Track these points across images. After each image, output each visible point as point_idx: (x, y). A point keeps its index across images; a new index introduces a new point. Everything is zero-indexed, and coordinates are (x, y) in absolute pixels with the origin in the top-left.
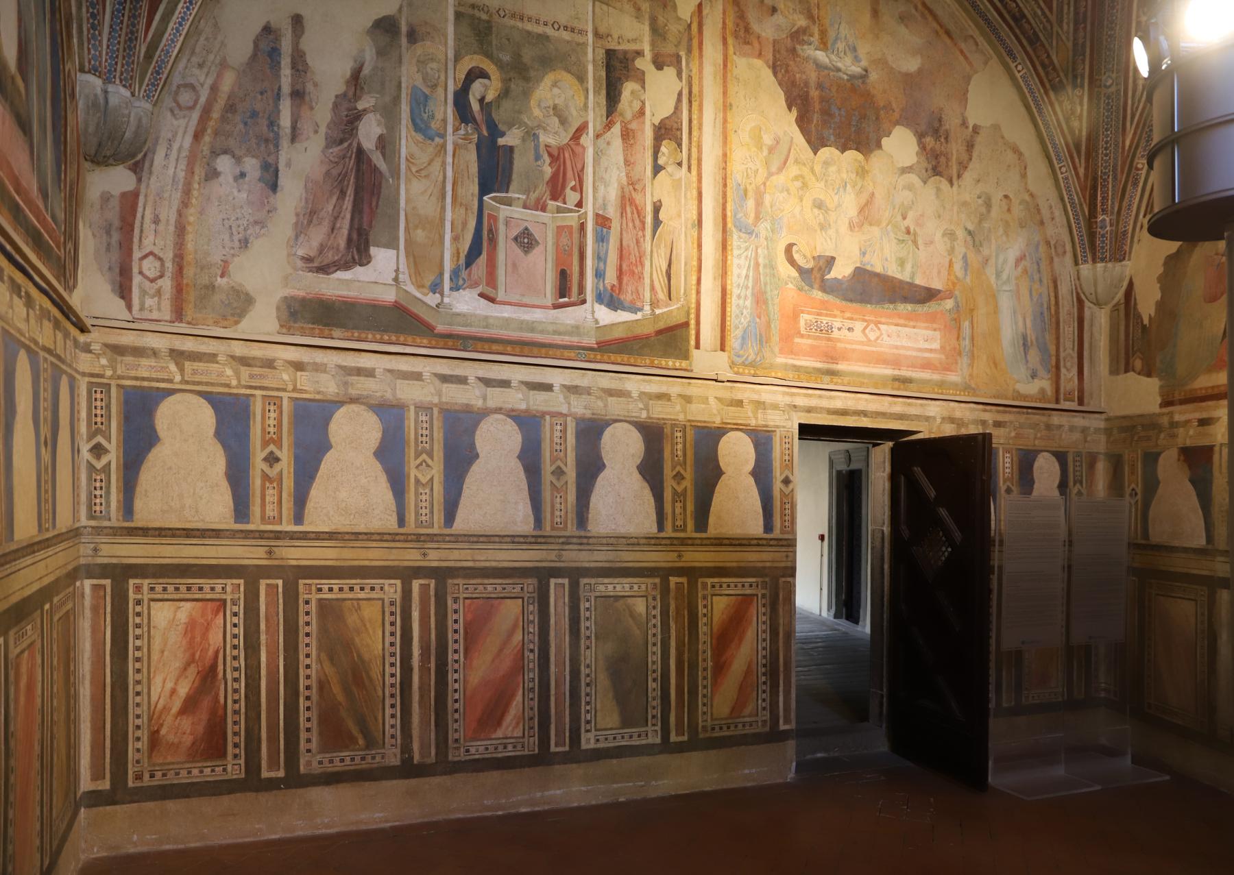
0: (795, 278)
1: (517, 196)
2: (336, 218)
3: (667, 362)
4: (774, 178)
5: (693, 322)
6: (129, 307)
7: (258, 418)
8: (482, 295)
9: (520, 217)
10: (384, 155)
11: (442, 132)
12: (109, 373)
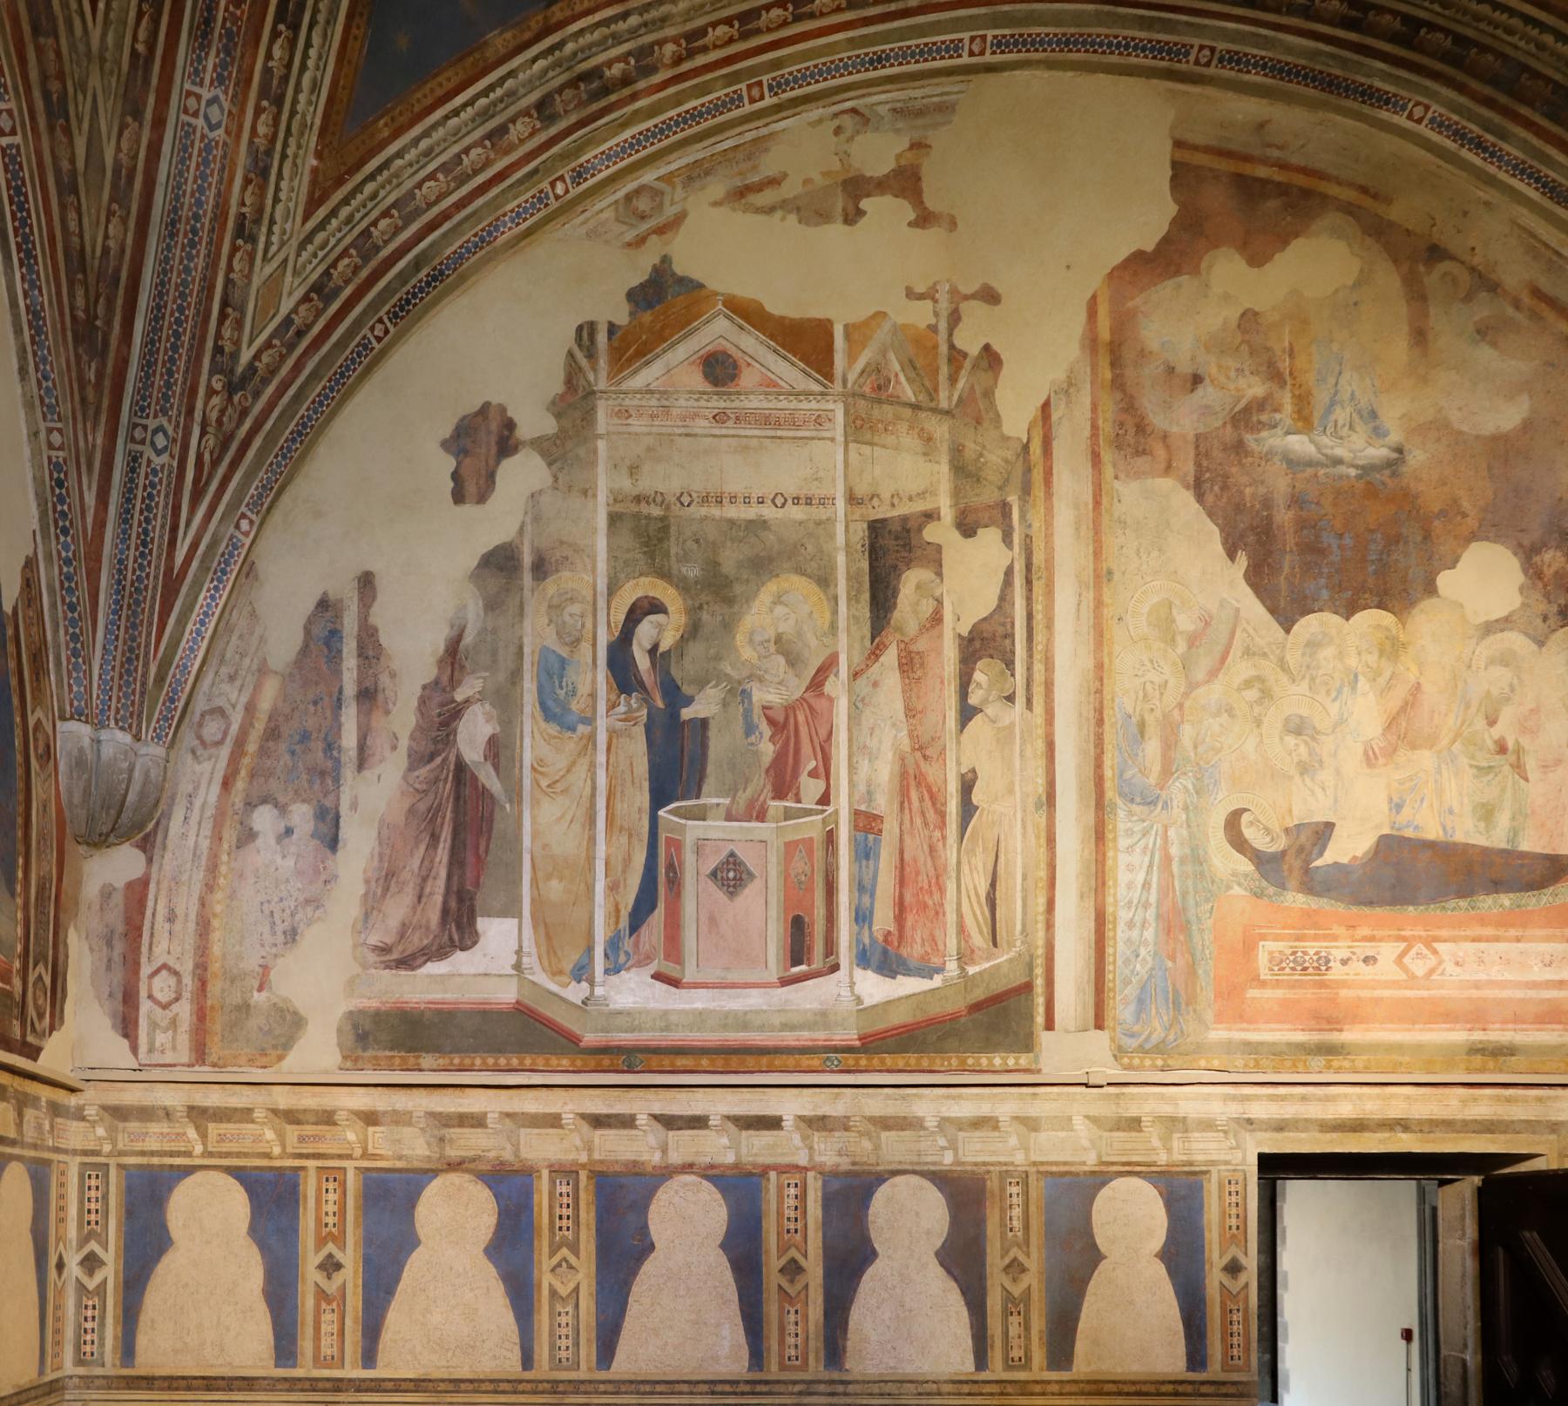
0: (1246, 875)
1: (715, 801)
2: (425, 879)
3: (990, 1060)
4: (1201, 691)
5: (1039, 983)
6: (134, 1049)
7: (311, 1203)
9: (721, 836)
10: (496, 768)
11: (589, 715)
12: (107, 1148)
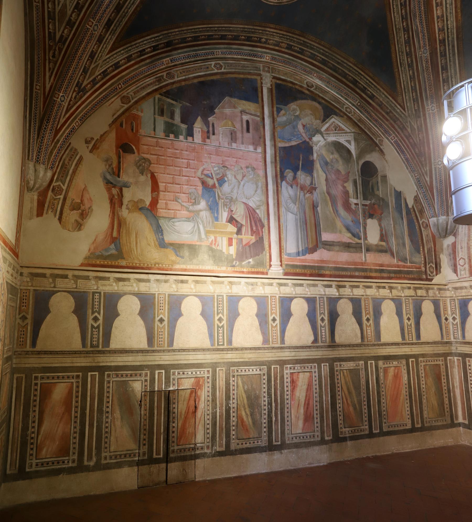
6: (457, 275)
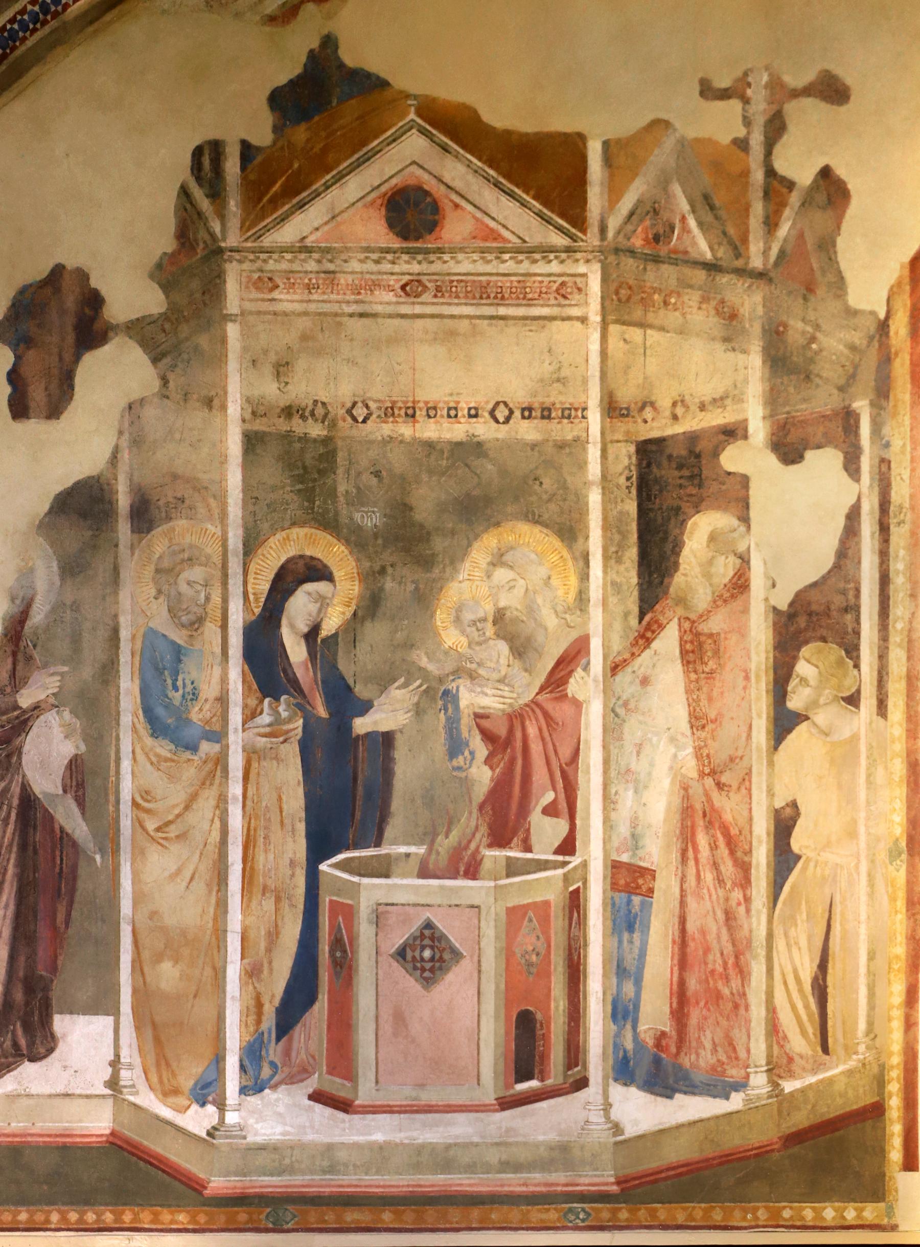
1: (403, 849)
8: (317, 1097)
9: (413, 899)
11: (217, 727)
